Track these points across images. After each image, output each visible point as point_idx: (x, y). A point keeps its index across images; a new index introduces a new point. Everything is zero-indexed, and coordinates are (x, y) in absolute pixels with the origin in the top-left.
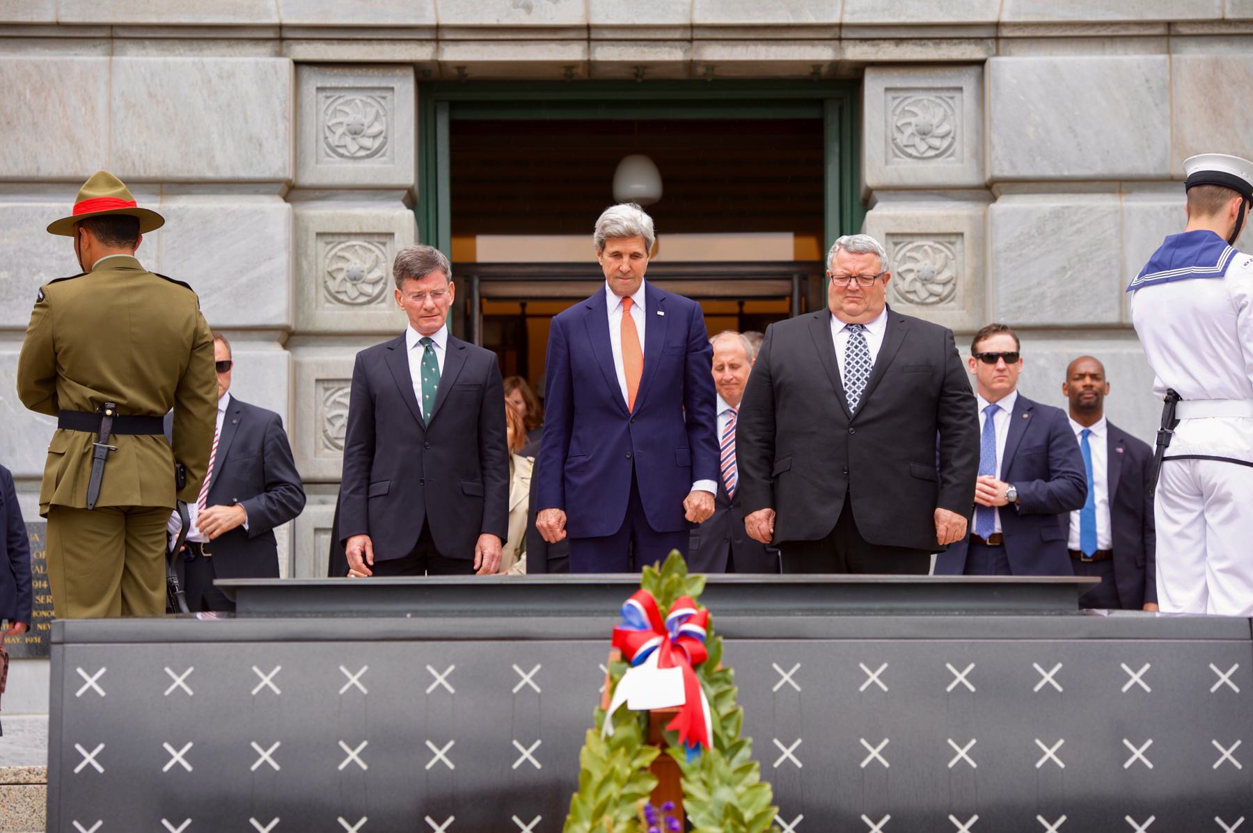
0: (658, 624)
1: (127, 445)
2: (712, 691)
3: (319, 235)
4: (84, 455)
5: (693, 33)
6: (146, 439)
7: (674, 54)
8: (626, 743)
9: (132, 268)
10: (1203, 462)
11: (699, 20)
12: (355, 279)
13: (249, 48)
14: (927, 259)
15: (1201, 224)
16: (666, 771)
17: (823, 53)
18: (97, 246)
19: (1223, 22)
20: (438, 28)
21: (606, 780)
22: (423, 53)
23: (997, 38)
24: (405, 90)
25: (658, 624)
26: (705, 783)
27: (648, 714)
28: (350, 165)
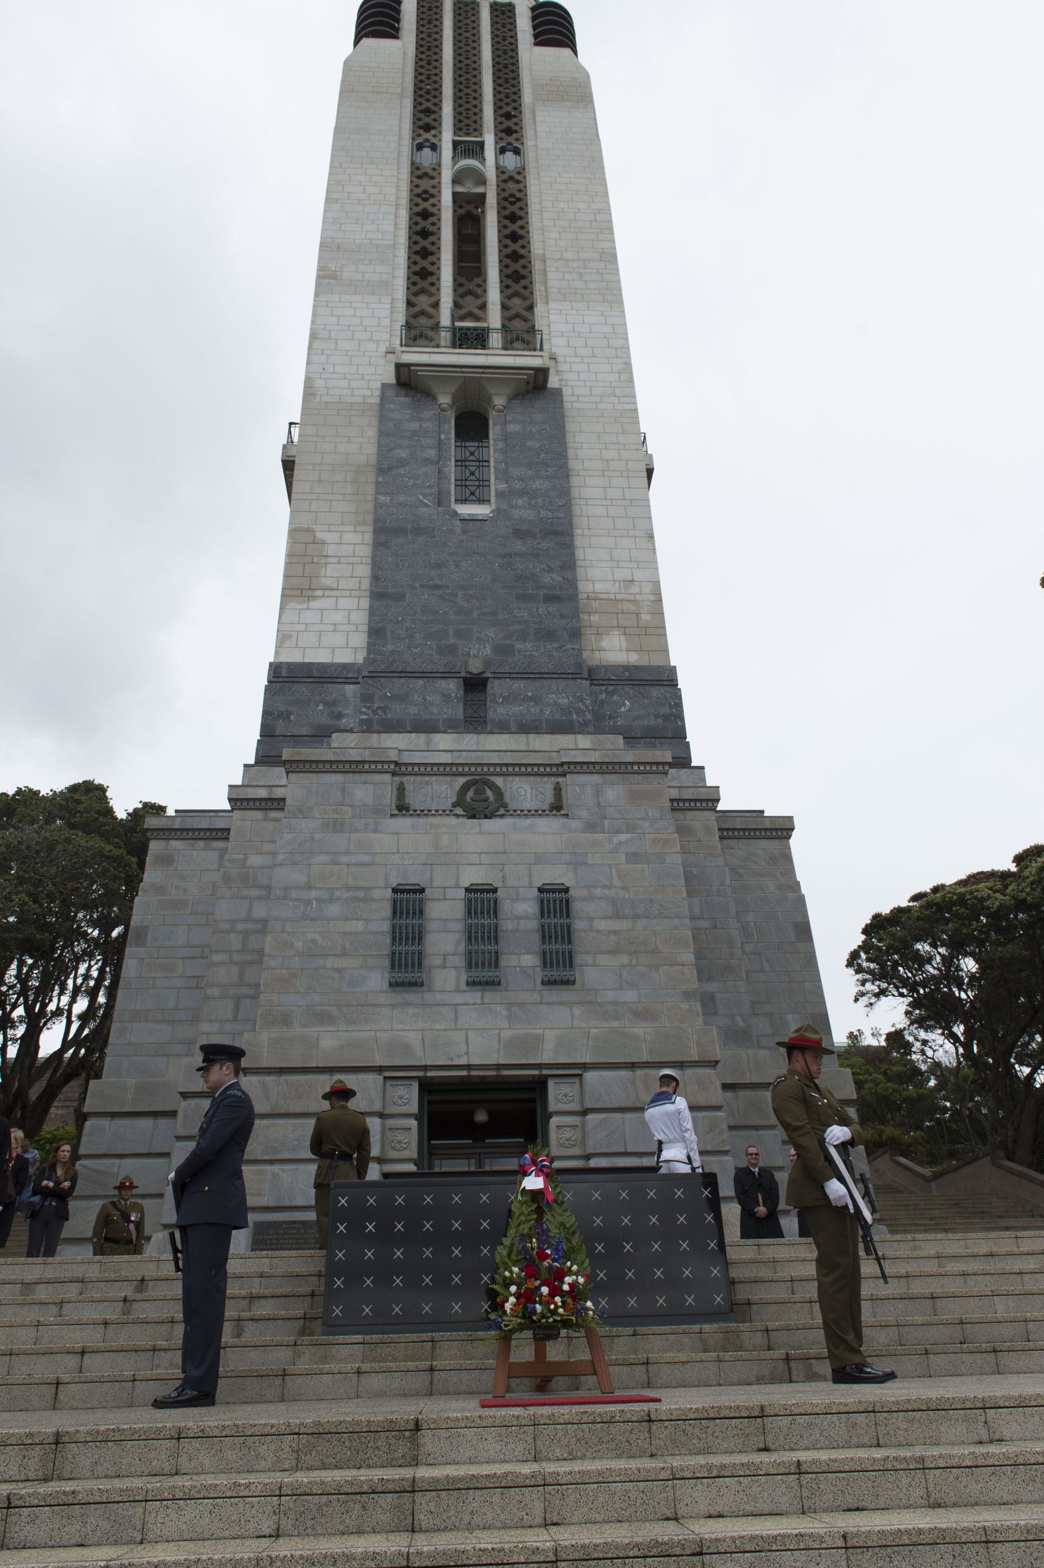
0: (534, 1162)
1: (341, 1163)
2: (553, 1185)
3: (390, 1129)
4: (328, 1167)
5: (499, 1067)
6: (348, 1163)
7: (493, 1073)
8: (526, 1202)
9: (346, 1108)
10: (671, 1163)
11: (501, 1062)
12: (399, 1142)
13: (371, 1073)
14: (568, 1133)
15: (665, 1089)
16: (540, 1212)
17: (536, 1072)
18: (336, 1101)
19: (647, 1063)
20: (426, 1066)
21: (520, 1215)
22: (421, 1074)
23: (585, 1068)
24: (415, 1086)
25: (534, 1162)
26: (553, 1215)
27: (532, 1191)
28: (399, 1108)
